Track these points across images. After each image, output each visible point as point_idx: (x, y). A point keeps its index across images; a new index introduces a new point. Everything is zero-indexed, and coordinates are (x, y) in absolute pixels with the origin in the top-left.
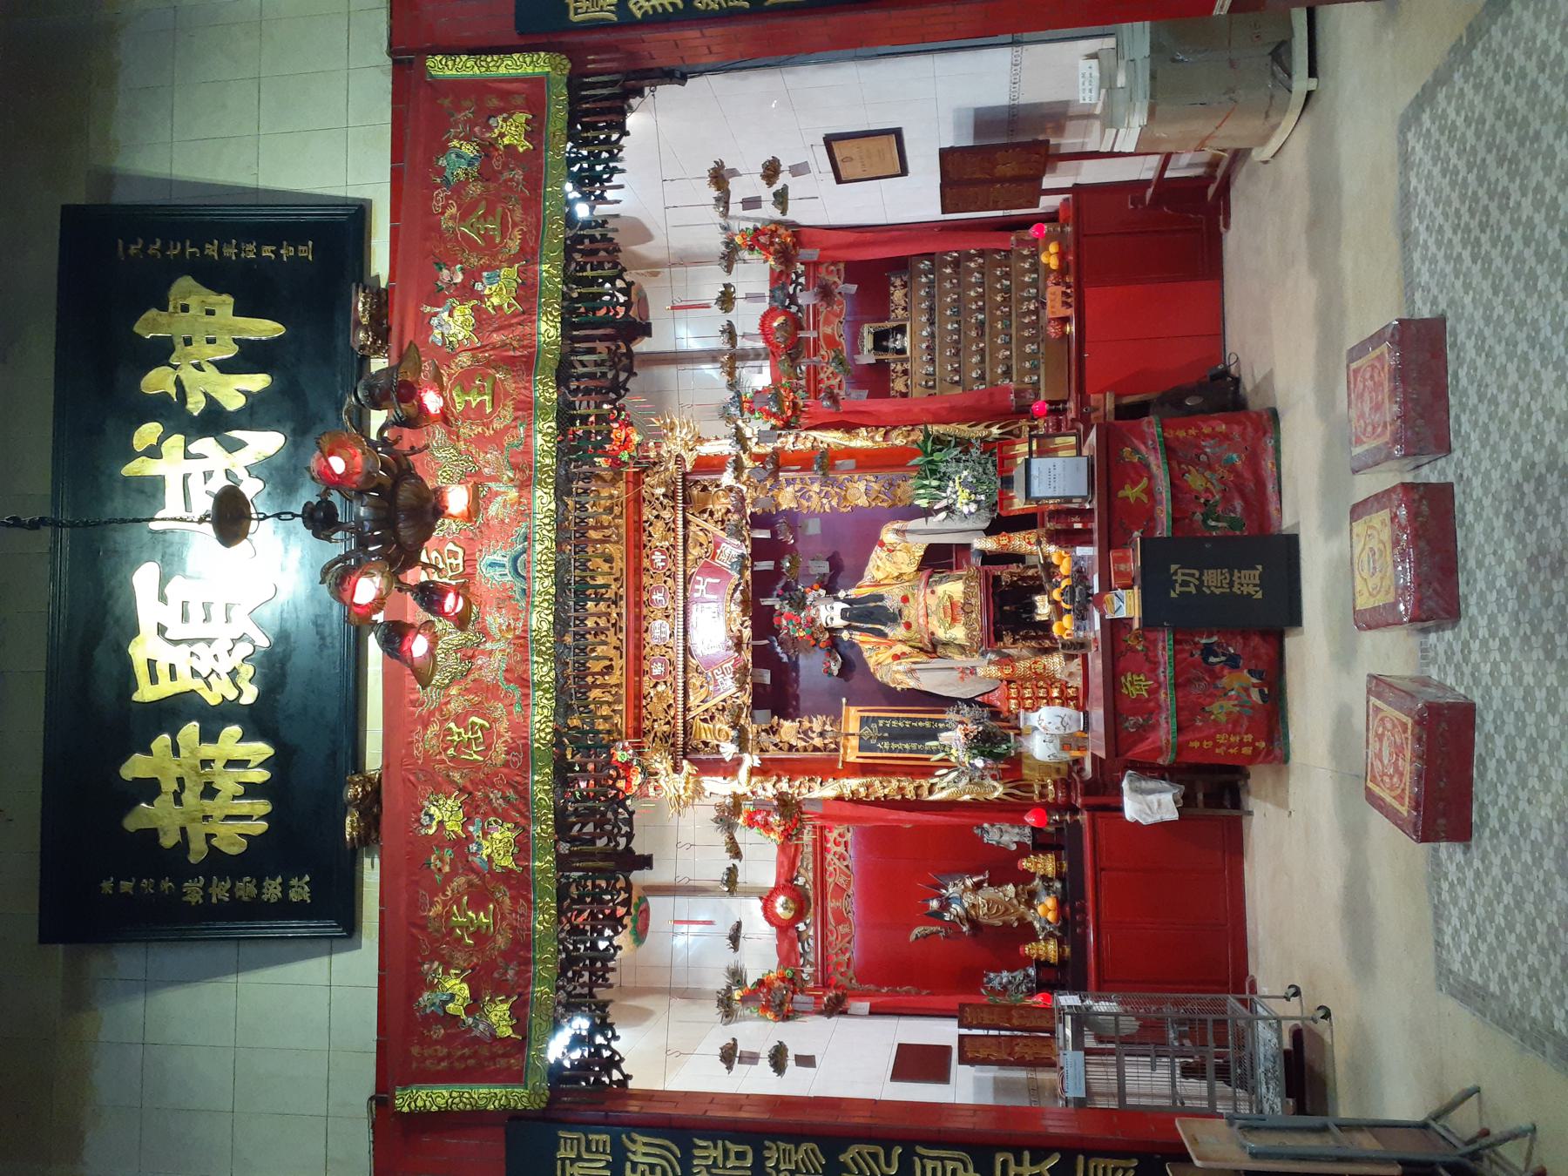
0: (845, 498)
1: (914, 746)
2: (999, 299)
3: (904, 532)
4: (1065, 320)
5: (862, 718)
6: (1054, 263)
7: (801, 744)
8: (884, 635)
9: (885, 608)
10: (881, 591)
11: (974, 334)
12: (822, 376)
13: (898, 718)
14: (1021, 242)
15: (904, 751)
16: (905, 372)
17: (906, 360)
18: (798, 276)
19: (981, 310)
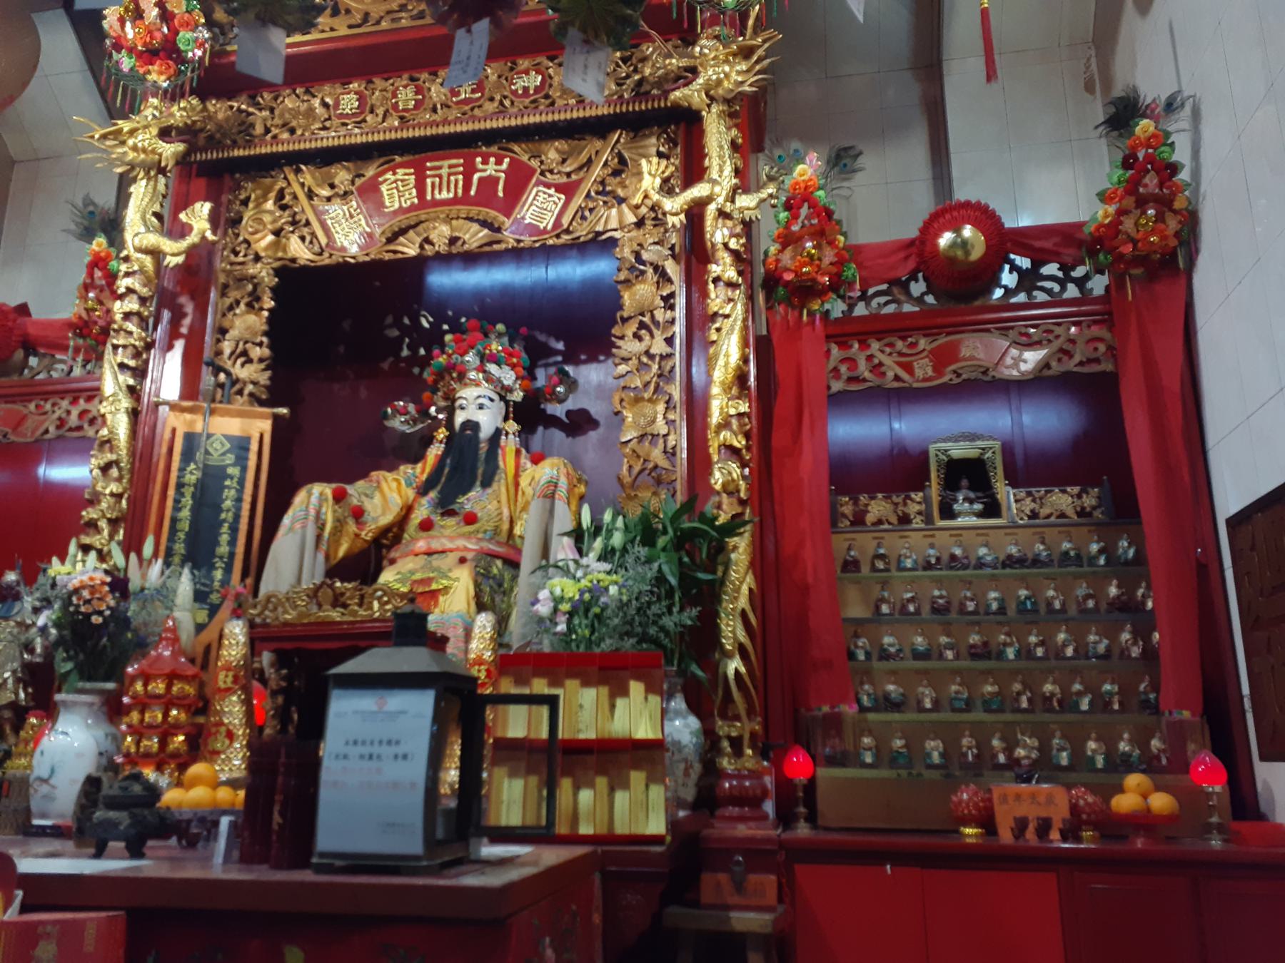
0: (638, 400)
1: (185, 526)
2: (1048, 688)
3: (552, 497)
4: (987, 822)
5: (247, 440)
6: (1125, 802)
7: (227, 347)
8: (423, 490)
9: (466, 490)
10: (500, 486)
11: (974, 639)
12: (875, 346)
13: (240, 496)
14: (1177, 735)
15: (177, 507)
16: (905, 520)
17: (929, 520)
18: (1081, 282)
19: (1025, 653)
